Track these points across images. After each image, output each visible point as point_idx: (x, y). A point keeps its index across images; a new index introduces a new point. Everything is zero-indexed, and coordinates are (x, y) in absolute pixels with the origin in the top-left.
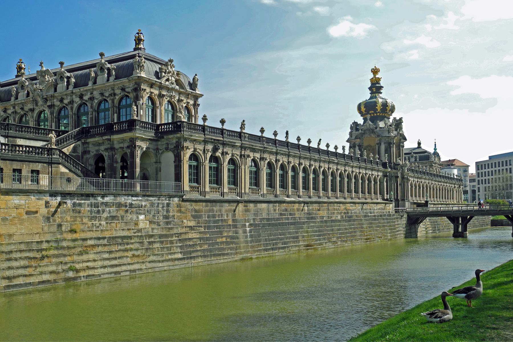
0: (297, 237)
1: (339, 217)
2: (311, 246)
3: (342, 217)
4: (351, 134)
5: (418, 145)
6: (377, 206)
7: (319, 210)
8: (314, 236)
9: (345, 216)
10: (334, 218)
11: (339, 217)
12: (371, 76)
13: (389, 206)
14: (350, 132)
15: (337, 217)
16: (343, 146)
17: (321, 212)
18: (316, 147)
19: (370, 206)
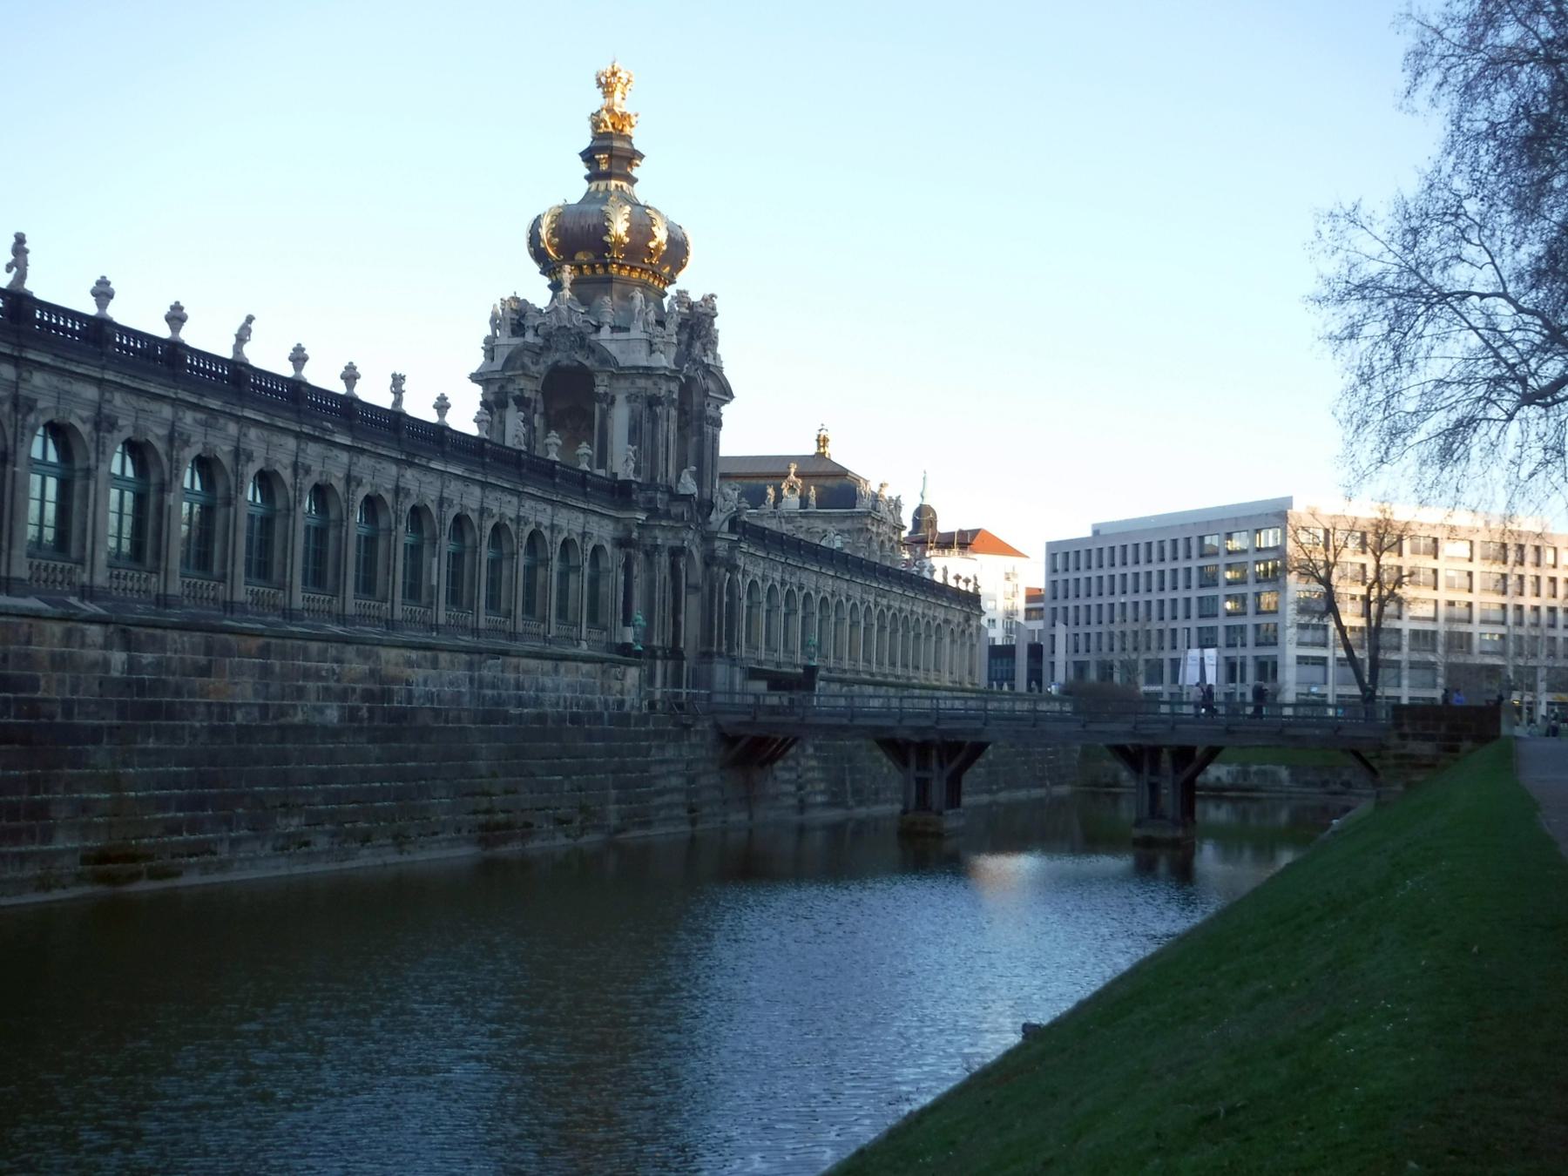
0: (40, 811)
1: (332, 715)
2: (132, 858)
3: (352, 715)
4: (490, 347)
5: (819, 447)
6: (556, 671)
7: (205, 671)
8: (162, 804)
9: (370, 710)
10: (299, 718)
11: (332, 715)
12: (596, 101)
13: (624, 675)
14: (488, 337)
15: (321, 711)
16: (394, 376)
17: (213, 682)
18: (228, 354)
19: (517, 668)
